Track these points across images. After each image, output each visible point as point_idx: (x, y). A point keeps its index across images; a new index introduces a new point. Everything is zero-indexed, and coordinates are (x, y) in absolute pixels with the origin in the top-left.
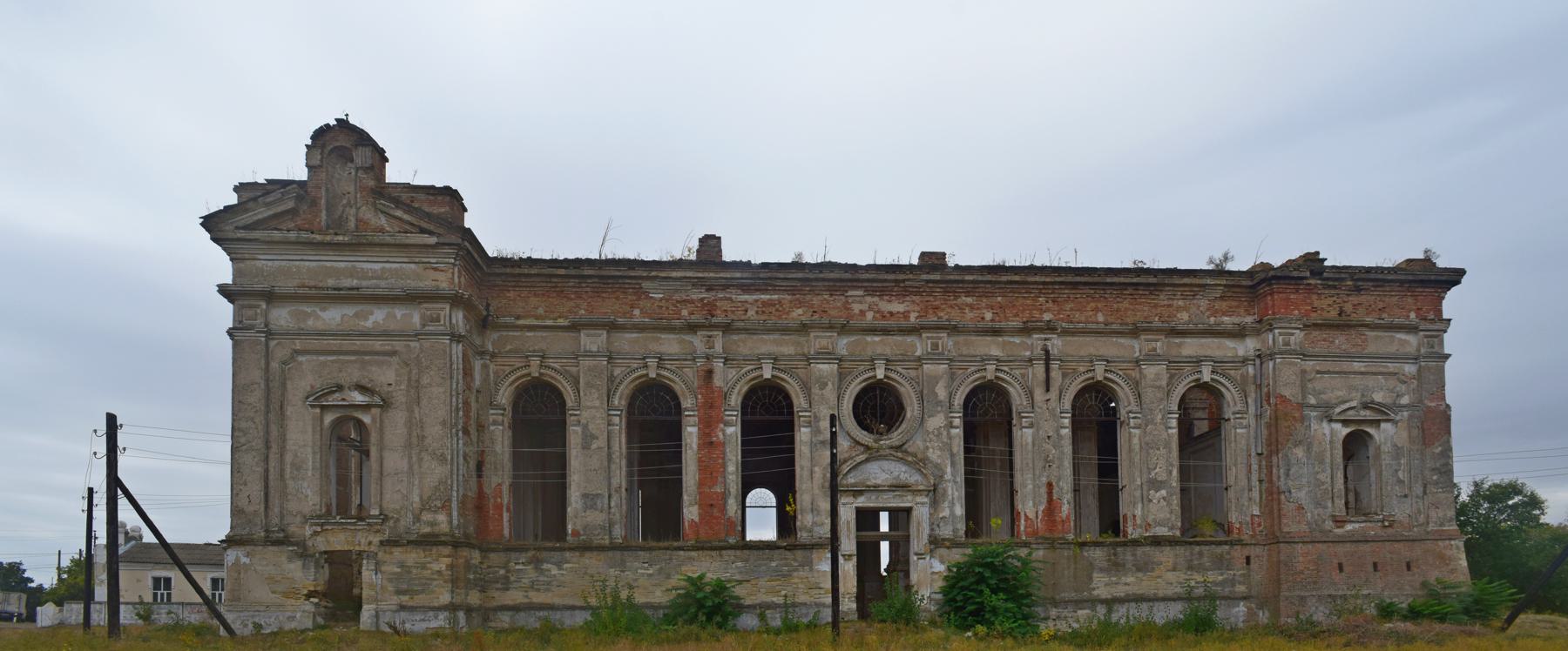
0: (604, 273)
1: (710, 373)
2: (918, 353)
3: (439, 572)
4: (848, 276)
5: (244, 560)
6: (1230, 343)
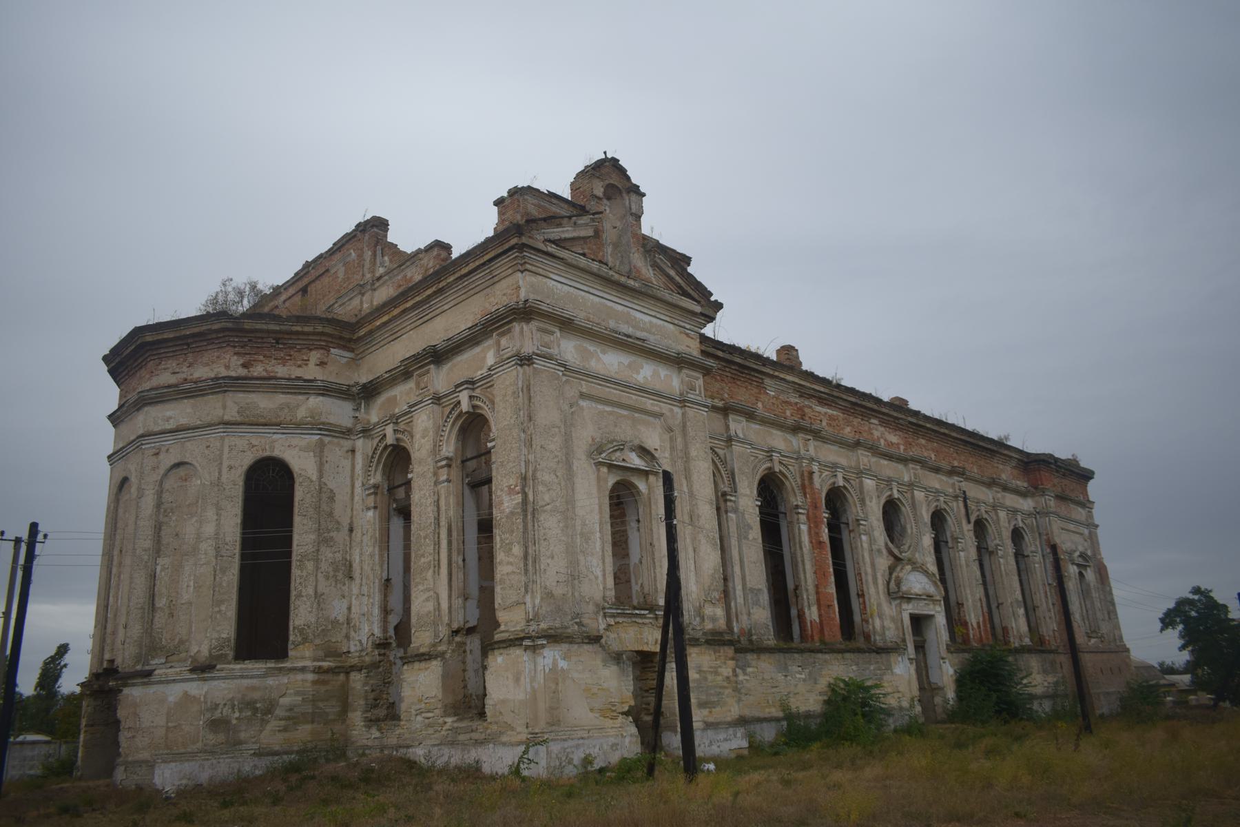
0: (747, 364)
1: (811, 473)
2: (906, 479)
3: (728, 678)
4: (875, 407)
5: (562, 664)
6: (1021, 500)
